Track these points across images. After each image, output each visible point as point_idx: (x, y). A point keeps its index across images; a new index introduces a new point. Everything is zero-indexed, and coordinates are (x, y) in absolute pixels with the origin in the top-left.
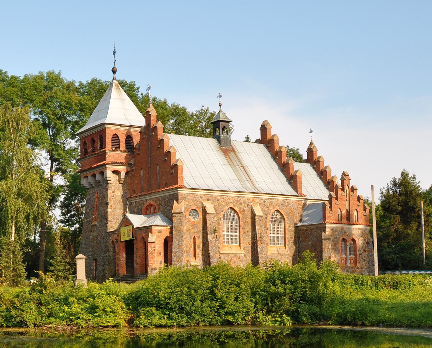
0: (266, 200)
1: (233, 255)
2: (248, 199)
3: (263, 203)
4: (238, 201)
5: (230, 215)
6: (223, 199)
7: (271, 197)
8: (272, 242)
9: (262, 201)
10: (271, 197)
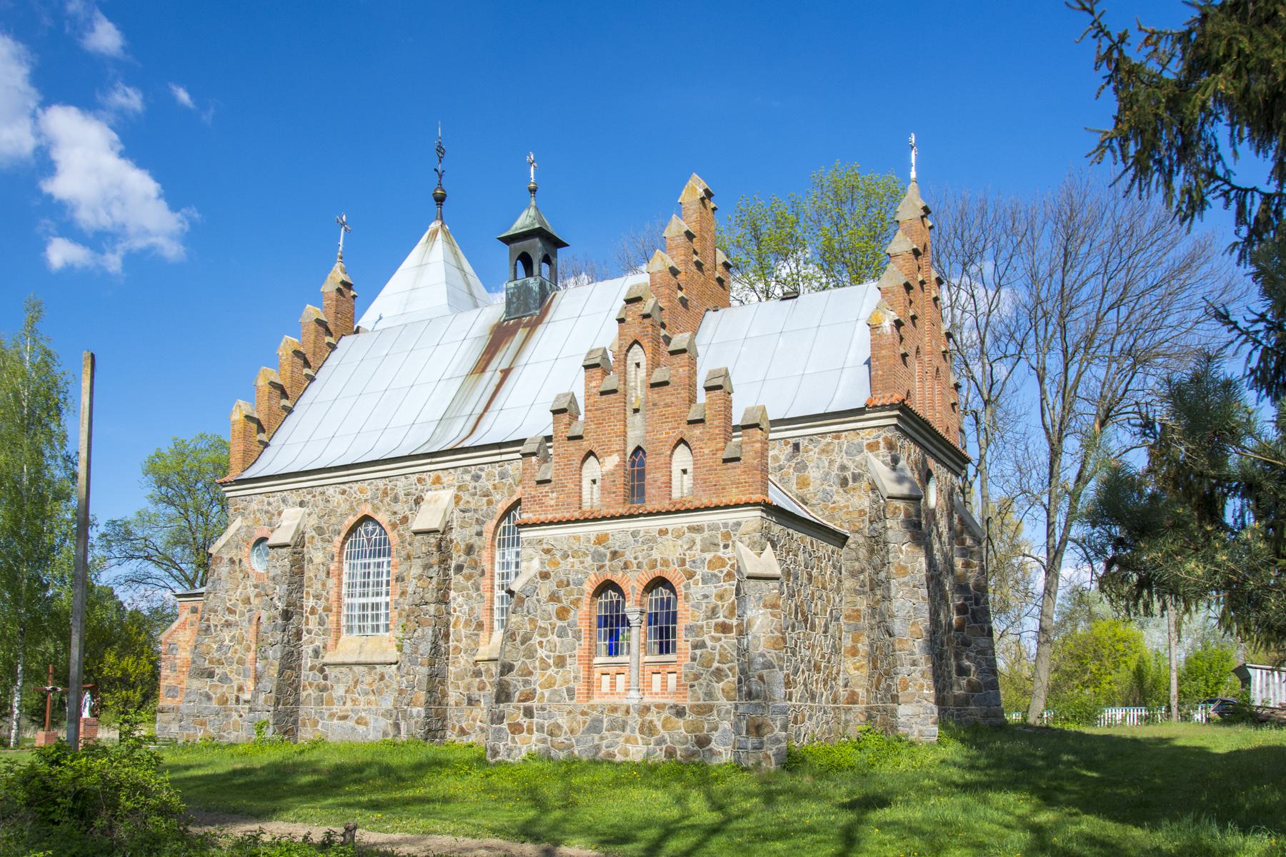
0: (481, 470)
1: (362, 668)
2: (419, 480)
3: (473, 484)
4: (385, 493)
5: (369, 540)
6: (344, 492)
7: (497, 458)
8: (356, 623)
9: (467, 477)
10: (497, 458)
